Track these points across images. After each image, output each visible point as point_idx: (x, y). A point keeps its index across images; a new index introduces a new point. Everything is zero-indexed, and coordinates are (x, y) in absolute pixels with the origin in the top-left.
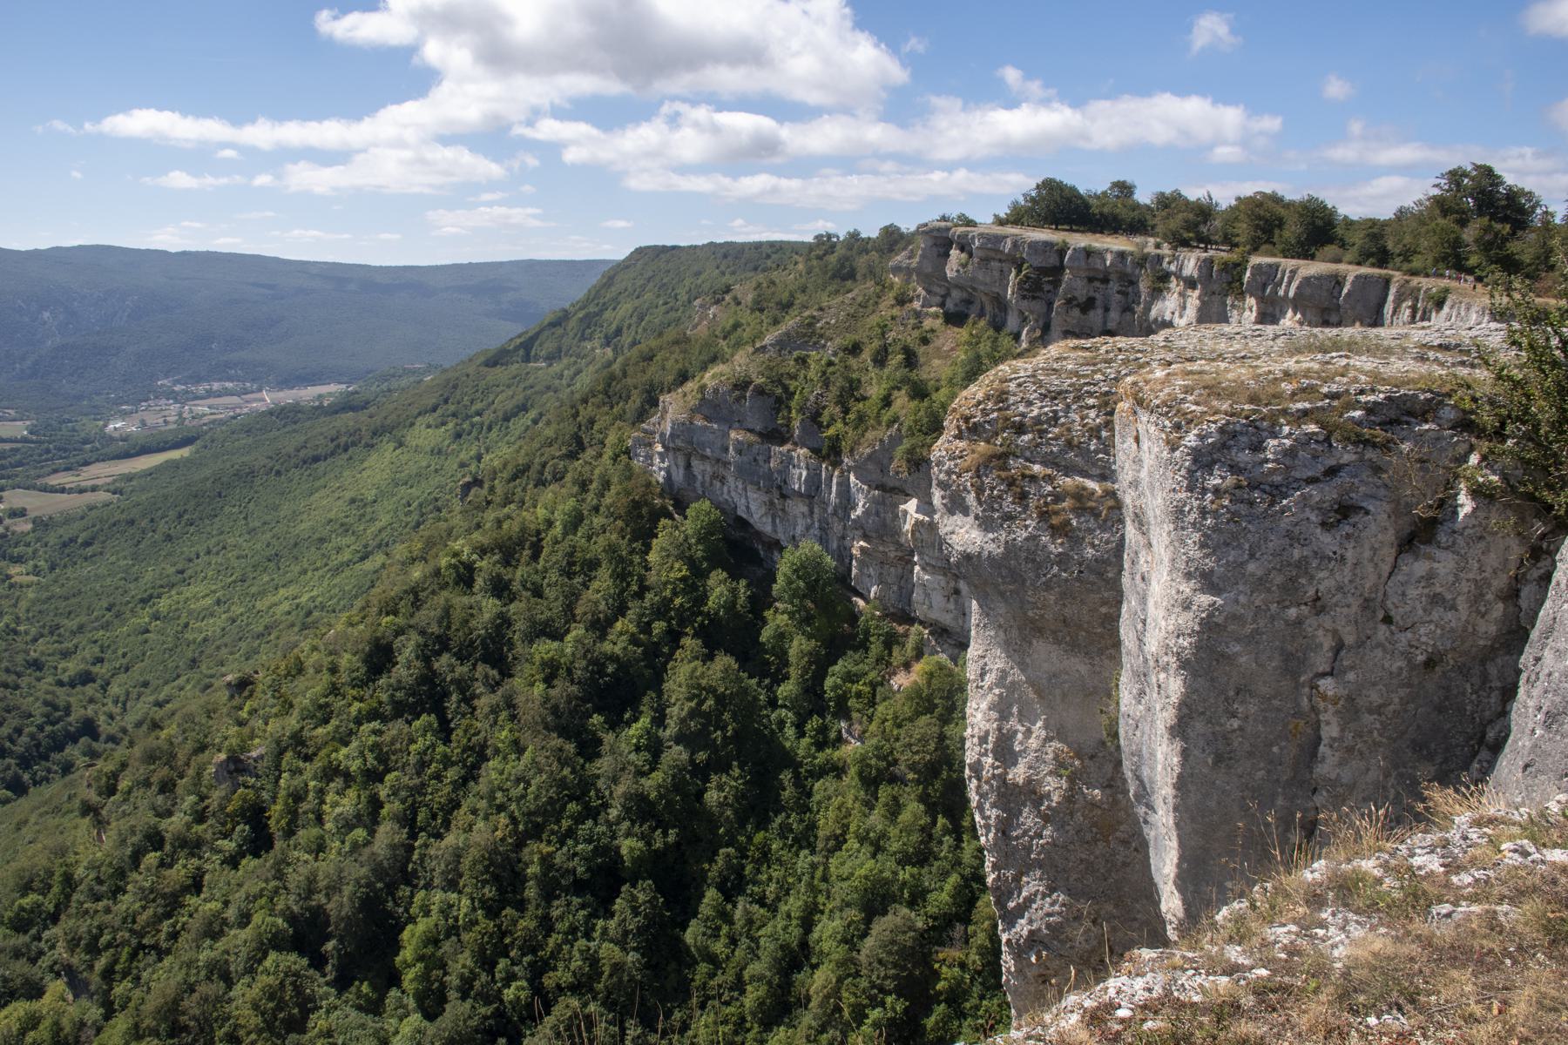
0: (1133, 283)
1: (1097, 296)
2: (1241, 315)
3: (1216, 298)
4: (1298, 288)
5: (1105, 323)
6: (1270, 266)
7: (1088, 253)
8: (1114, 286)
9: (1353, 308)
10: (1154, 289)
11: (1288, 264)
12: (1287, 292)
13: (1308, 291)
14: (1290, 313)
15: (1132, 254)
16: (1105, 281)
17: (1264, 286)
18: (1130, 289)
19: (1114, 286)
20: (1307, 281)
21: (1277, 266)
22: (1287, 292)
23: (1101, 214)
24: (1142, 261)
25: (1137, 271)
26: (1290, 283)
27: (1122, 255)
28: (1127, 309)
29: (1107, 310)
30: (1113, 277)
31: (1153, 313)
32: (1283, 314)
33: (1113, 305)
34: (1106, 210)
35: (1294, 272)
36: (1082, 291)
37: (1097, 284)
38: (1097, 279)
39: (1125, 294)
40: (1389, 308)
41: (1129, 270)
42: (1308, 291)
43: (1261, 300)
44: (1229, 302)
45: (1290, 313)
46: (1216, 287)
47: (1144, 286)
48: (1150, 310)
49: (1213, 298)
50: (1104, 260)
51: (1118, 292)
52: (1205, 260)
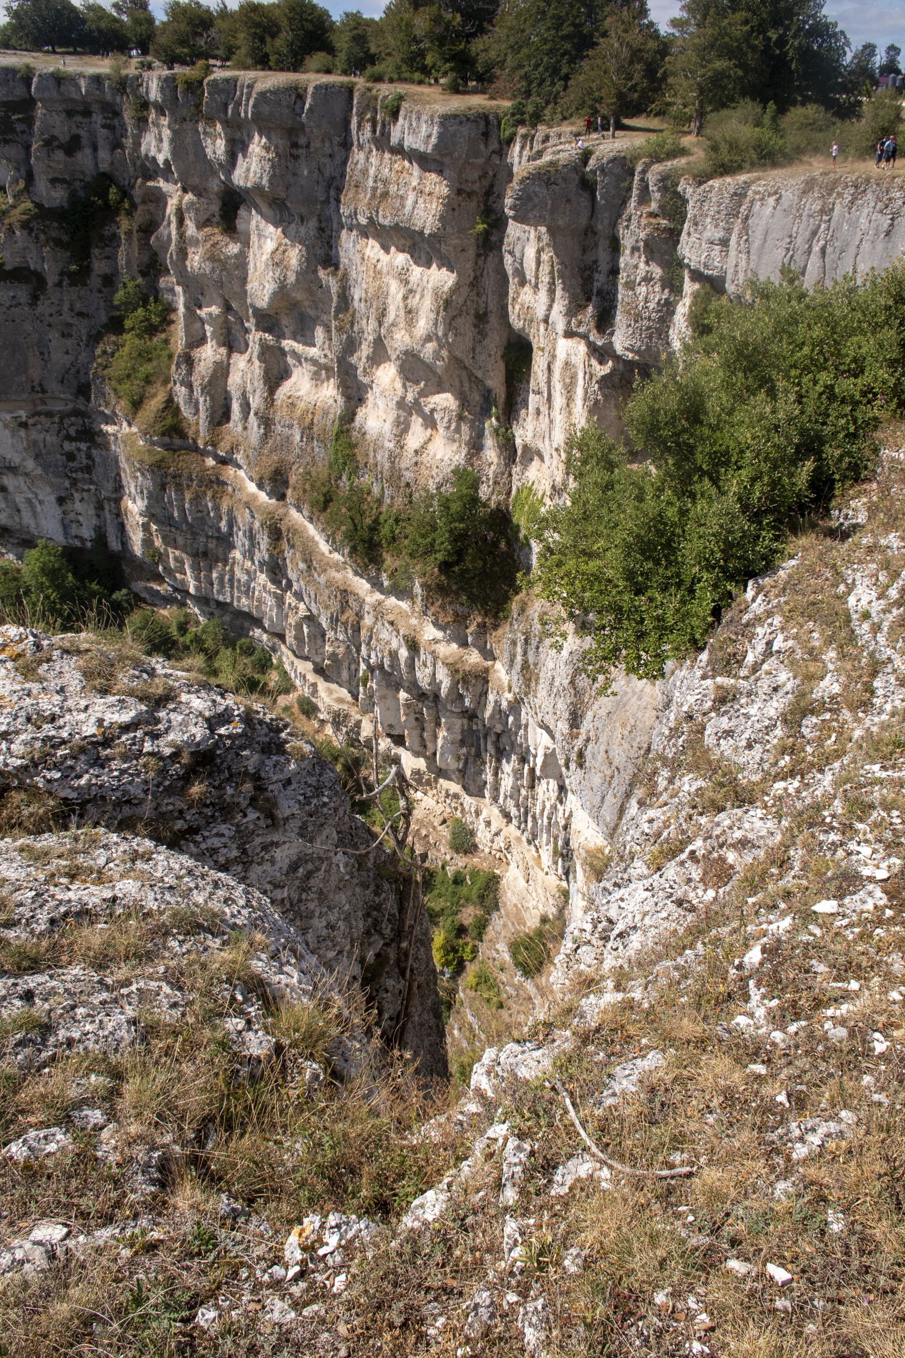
0: (117, 114)
1: (82, 133)
2: (214, 143)
3: (188, 125)
4: (254, 106)
5: (96, 164)
6: (227, 81)
7: (59, 79)
8: (98, 119)
9: (319, 126)
10: (139, 119)
11: (246, 76)
12: (246, 113)
13: (266, 109)
14: (257, 137)
15: (108, 77)
16: (87, 113)
17: (226, 106)
18: (116, 122)
19: (98, 119)
20: (262, 94)
21: (235, 80)
22: (246, 113)
23: (100, 31)
24: (123, 85)
25: (118, 99)
26: (248, 100)
27: (97, 79)
28: (117, 145)
29: (95, 149)
30: (95, 107)
31: (143, 149)
32: (251, 138)
33: (101, 143)
34: (103, 25)
35: (251, 87)
36: (62, 129)
37: (79, 118)
38: (77, 112)
39: (110, 127)
40: (354, 121)
41: (109, 97)
42: (266, 109)
43: (226, 124)
44: (200, 129)
45: (257, 137)
46: (185, 112)
47: (128, 116)
48: (140, 145)
49: (185, 125)
50: (78, 87)
51: (103, 126)
52: (167, 79)
